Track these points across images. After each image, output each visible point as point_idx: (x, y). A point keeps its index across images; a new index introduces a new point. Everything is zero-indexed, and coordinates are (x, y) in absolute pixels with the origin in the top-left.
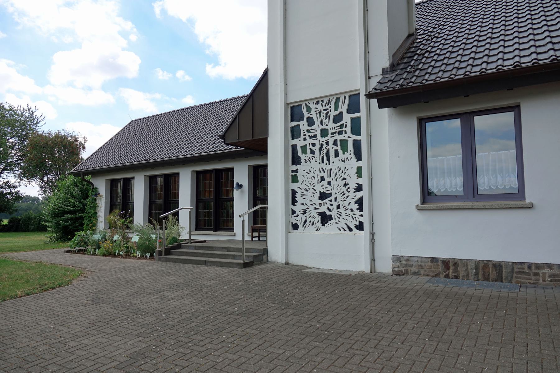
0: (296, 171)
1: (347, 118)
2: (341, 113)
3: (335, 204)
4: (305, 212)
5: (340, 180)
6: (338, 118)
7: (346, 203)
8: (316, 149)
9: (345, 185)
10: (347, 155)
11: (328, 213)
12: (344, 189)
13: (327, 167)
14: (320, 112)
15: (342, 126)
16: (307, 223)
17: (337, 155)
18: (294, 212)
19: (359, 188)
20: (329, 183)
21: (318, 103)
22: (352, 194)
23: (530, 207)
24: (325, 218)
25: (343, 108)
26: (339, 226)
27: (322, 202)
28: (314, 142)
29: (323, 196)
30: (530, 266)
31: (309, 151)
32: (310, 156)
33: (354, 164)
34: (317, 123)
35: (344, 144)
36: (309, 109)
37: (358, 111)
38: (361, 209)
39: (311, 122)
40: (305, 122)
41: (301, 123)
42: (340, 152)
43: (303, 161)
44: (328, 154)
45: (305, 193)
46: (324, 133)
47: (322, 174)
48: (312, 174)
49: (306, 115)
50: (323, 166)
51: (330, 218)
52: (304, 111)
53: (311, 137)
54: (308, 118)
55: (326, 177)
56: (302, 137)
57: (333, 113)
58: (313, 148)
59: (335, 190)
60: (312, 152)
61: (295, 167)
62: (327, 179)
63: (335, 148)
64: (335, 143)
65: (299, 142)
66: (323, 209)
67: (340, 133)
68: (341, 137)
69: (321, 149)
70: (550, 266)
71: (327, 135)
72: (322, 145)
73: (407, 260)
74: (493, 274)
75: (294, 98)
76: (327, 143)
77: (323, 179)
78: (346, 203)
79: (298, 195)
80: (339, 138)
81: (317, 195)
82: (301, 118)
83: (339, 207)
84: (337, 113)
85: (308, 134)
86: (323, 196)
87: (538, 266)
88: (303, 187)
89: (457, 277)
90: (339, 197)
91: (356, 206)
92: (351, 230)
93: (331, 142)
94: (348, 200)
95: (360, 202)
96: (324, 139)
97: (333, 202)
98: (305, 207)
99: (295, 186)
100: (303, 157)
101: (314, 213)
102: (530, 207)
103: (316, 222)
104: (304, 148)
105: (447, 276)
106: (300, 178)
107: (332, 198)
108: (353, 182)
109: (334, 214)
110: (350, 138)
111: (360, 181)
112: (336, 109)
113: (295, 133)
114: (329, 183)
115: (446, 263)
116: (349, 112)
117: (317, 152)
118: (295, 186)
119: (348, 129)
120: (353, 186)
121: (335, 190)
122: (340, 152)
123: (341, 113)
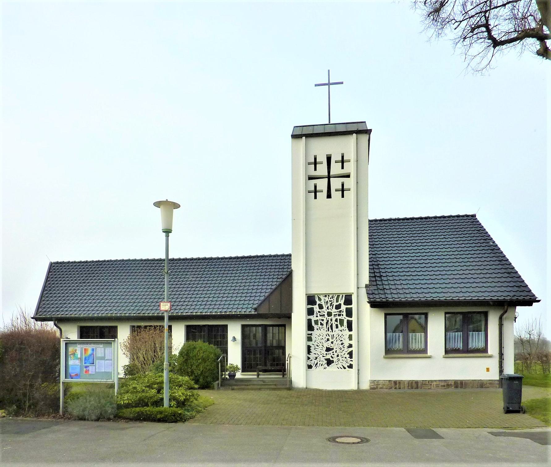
0: (311, 334)
1: (344, 307)
2: (340, 304)
3: (336, 354)
4: (316, 358)
5: (339, 341)
6: (338, 307)
7: (342, 354)
8: (324, 323)
9: (342, 344)
10: (343, 328)
11: (331, 359)
12: (341, 346)
13: (330, 333)
14: (327, 302)
15: (340, 311)
16: (318, 365)
17: (337, 327)
18: (309, 358)
19: (350, 346)
20: (332, 343)
21: (326, 296)
22: (346, 349)
23: (430, 357)
24: (329, 362)
25: (342, 302)
26: (338, 366)
27: (328, 353)
28: (323, 318)
29: (328, 349)
30: (429, 381)
31: (319, 323)
32: (321, 326)
33: (347, 333)
34: (325, 308)
35: (342, 322)
36: (320, 299)
37: (351, 304)
38: (351, 357)
39: (321, 307)
40: (317, 306)
41: (314, 306)
42: (339, 326)
43: (315, 329)
44: (331, 326)
45: (317, 347)
46: (329, 314)
47: (328, 337)
48: (321, 337)
49: (318, 302)
50: (329, 333)
51: (333, 362)
52: (317, 300)
53: (320, 316)
54: (319, 305)
55: (330, 339)
56: (315, 315)
57: (335, 304)
58: (322, 322)
59: (336, 346)
60: (322, 324)
61: (310, 332)
62: (331, 340)
63: (336, 323)
64: (336, 320)
65: (313, 318)
66: (328, 357)
67: (339, 315)
68: (340, 317)
69: (327, 323)
70: (435, 381)
71: (331, 316)
72: (328, 321)
73: (378, 382)
74: (414, 385)
75: (313, 291)
76: (331, 320)
77: (328, 340)
78: (342, 354)
79: (312, 349)
80: (339, 318)
81: (325, 349)
82: (314, 303)
83: (338, 356)
84: (338, 304)
85: (319, 314)
86: (328, 349)
87: (432, 381)
88: (316, 344)
89: (400, 388)
90: (338, 351)
91: (348, 356)
92: (345, 368)
93: (334, 319)
94: (344, 352)
95: (351, 354)
96: (330, 318)
97: (335, 353)
98: (317, 356)
99: (310, 343)
100: (316, 327)
101: (323, 359)
102: (430, 357)
103: (324, 364)
104: (316, 322)
105: (396, 388)
106: (313, 339)
107: (334, 351)
108: (347, 342)
109: (335, 359)
110: (346, 319)
111: (351, 342)
112: (337, 301)
113: (310, 312)
114: (332, 343)
115: (395, 382)
116: (345, 304)
117: (325, 325)
118: (310, 343)
119: (344, 313)
120: (346, 345)
121: (336, 347)
122: (339, 326)
123: (340, 304)
